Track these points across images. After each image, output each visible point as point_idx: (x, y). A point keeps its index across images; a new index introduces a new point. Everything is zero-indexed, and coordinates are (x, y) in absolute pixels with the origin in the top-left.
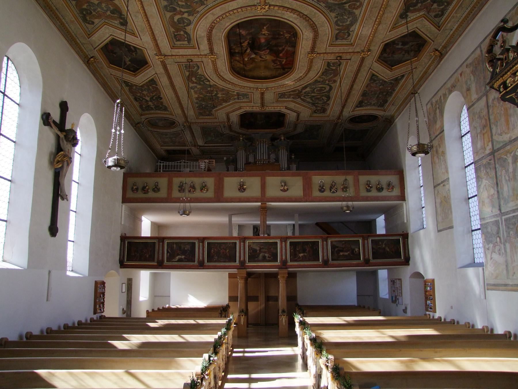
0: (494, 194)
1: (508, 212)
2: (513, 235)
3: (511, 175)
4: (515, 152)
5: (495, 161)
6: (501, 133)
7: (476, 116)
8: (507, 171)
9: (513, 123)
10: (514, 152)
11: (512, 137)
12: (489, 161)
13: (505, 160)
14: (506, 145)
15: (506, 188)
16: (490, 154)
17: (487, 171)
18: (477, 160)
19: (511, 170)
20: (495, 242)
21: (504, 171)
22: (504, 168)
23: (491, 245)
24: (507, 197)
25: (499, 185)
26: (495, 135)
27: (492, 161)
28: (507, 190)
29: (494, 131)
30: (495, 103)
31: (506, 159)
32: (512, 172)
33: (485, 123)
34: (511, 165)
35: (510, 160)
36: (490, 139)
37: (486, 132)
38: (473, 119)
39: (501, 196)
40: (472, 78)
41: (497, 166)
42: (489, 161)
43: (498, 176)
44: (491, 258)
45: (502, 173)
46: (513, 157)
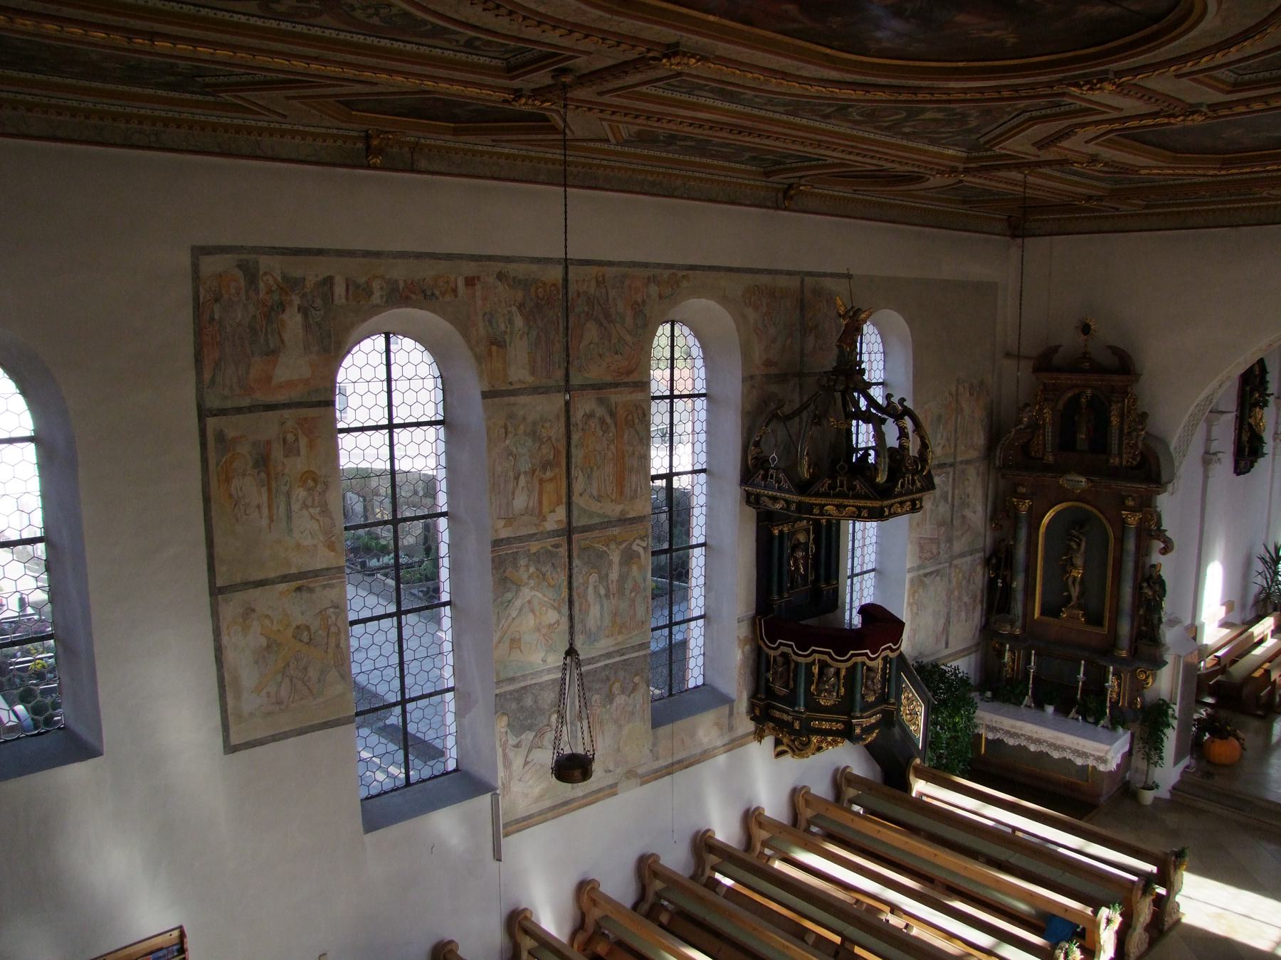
0: (558, 622)
1: (593, 658)
2: (599, 701)
3: (613, 587)
4: (631, 544)
5: (570, 551)
6: (600, 496)
7: (522, 427)
8: (604, 578)
9: (633, 486)
10: (627, 543)
11: (628, 513)
12: (550, 548)
13: (602, 556)
14: (608, 524)
15: (595, 611)
16: (555, 533)
17: (544, 570)
18: (508, 538)
19: (614, 575)
20: (542, 725)
21: (594, 578)
22: (596, 571)
23: (529, 736)
24: (594, 630)
25: (576, 605)
26: (581, 495)
27: (563, 551)
28: (598, 615)
29: (578, 486)
30: (593, 425)
31: (605, 552)
32: (618, 581)
33: (552, 457)
34: (616, 567)
35: (615, 557)
36: (564, 500)
37: (551, 480)
38: (506, 427)
39: (578, 627)
40: (519, 322)
41: (576, 562)
42: (550, 548)
43: (575, 584)
44: (526, 763)
45: (588, 582)
46: (623, 552)
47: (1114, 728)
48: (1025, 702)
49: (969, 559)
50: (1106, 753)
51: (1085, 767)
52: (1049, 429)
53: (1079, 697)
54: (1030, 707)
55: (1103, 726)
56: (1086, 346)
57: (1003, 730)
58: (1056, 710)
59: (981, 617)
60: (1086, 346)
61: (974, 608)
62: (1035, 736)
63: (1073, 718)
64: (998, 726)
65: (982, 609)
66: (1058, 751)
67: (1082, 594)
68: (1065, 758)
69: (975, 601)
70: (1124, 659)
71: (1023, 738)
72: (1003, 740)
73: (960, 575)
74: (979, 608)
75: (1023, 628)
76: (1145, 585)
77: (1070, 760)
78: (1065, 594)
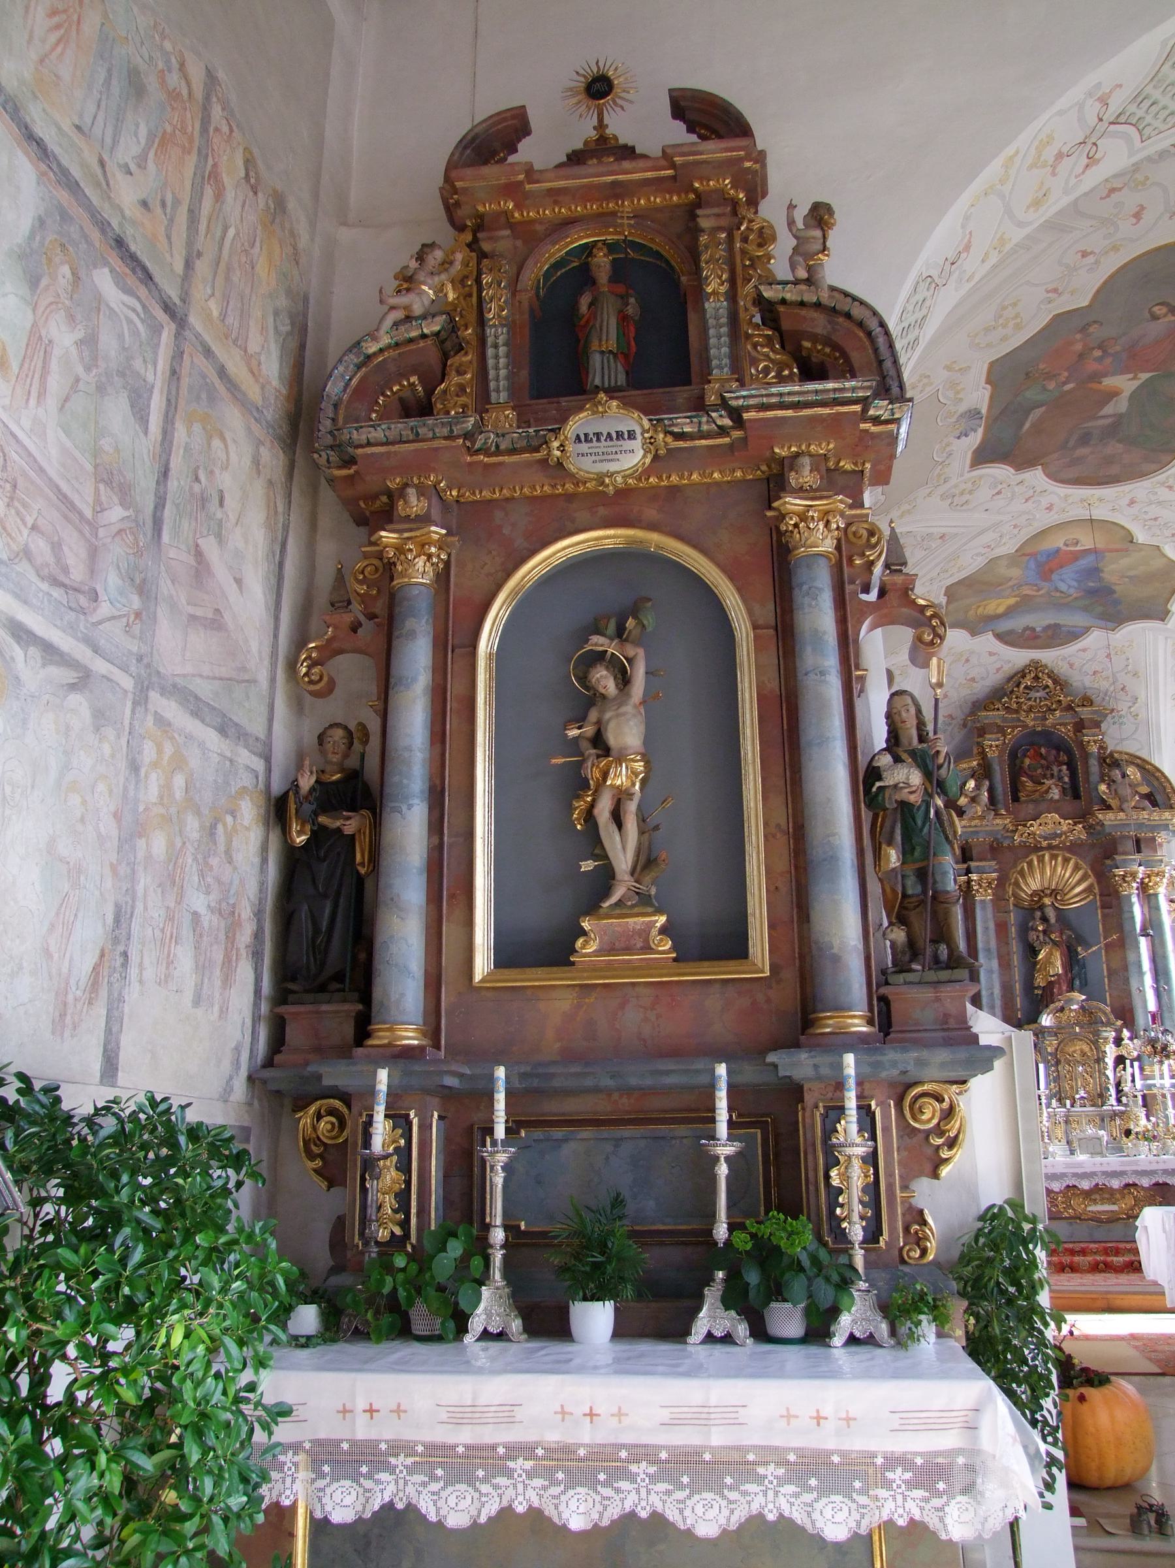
47: (901, 1339)
48: (477, 1324)
49: (211, 737)
50: (972, 1428)
51: (862, 1542)
52: (497, 334)
53: (721, 1232)
54: (501, 1336)
55: (852, 1340)
56: (601, 126)
57: (406, 1448)
58: (620, 1332)
59: (256, 1019)
60: (601, 126)
61: (228, 965)
62: (585, 1436)
63: (710, 1338)
64: (384, 1431)
65: (257, 992)
66: (719, 1489)
67: (646, 862)
68: (758, 1519)
69: (231, 938)
70: (862, 1038)
71: (520, 1465)
72: (411, 1508)
73: (179, 781)
74: (245, 972)
75: (433, 1032)
76: (886, 759)
77: (784, 1521)
78: (587, 866)
